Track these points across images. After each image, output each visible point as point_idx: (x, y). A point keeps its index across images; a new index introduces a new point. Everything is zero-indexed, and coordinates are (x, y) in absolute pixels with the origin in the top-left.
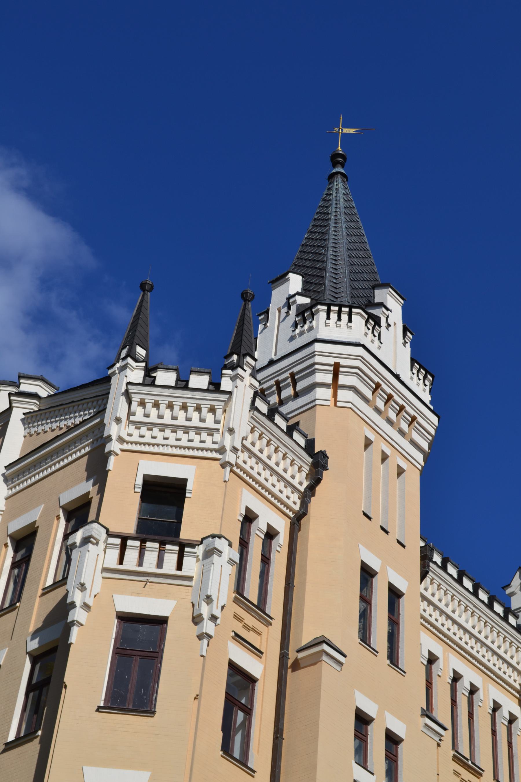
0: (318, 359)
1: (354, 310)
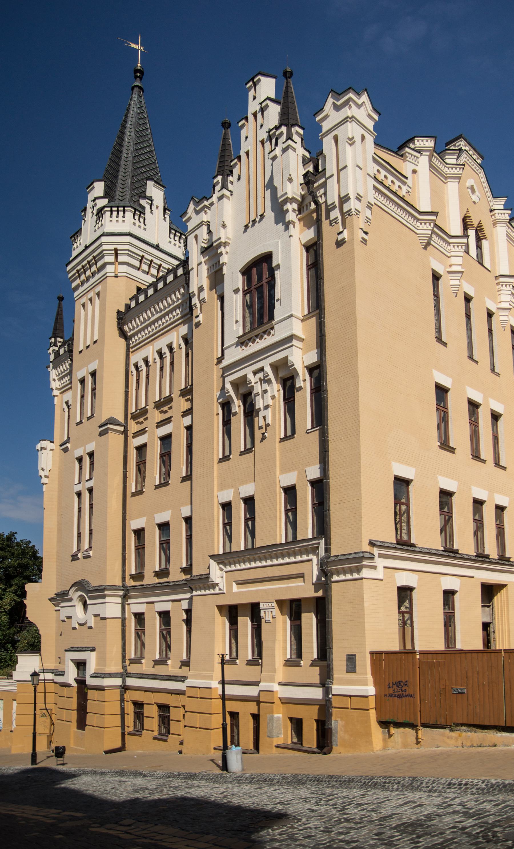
0: (104, 247)
1: (126, 209)
